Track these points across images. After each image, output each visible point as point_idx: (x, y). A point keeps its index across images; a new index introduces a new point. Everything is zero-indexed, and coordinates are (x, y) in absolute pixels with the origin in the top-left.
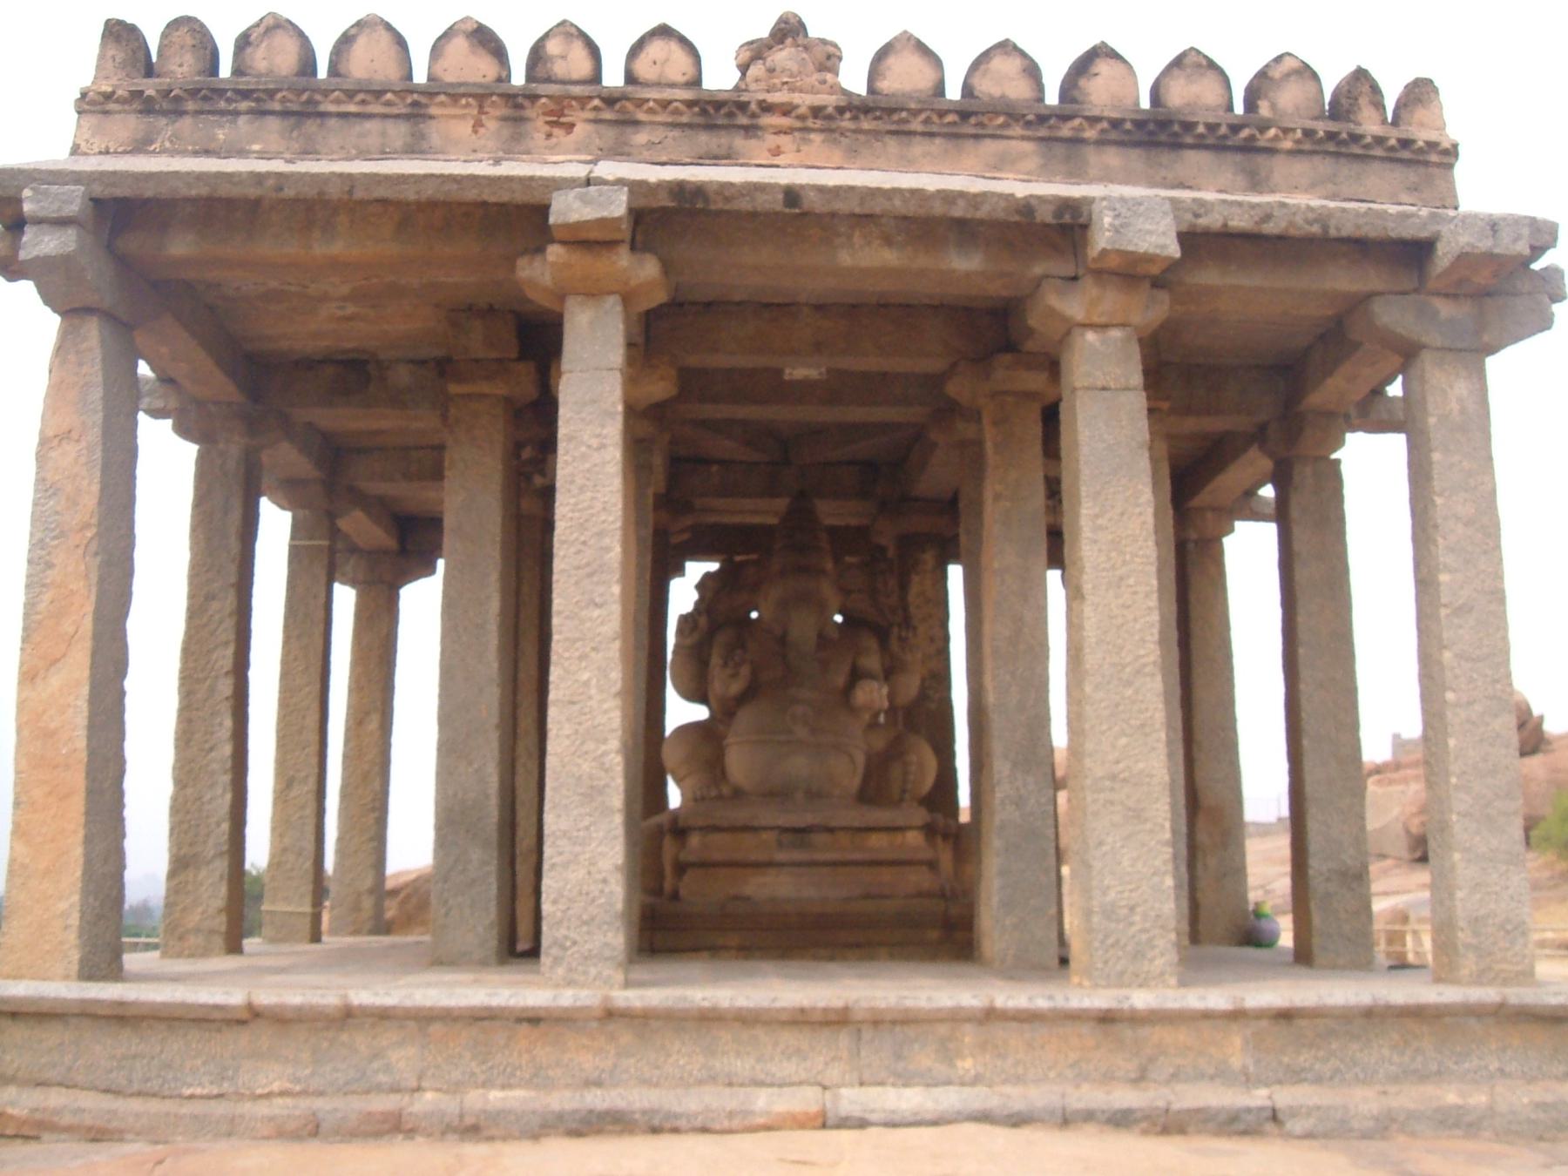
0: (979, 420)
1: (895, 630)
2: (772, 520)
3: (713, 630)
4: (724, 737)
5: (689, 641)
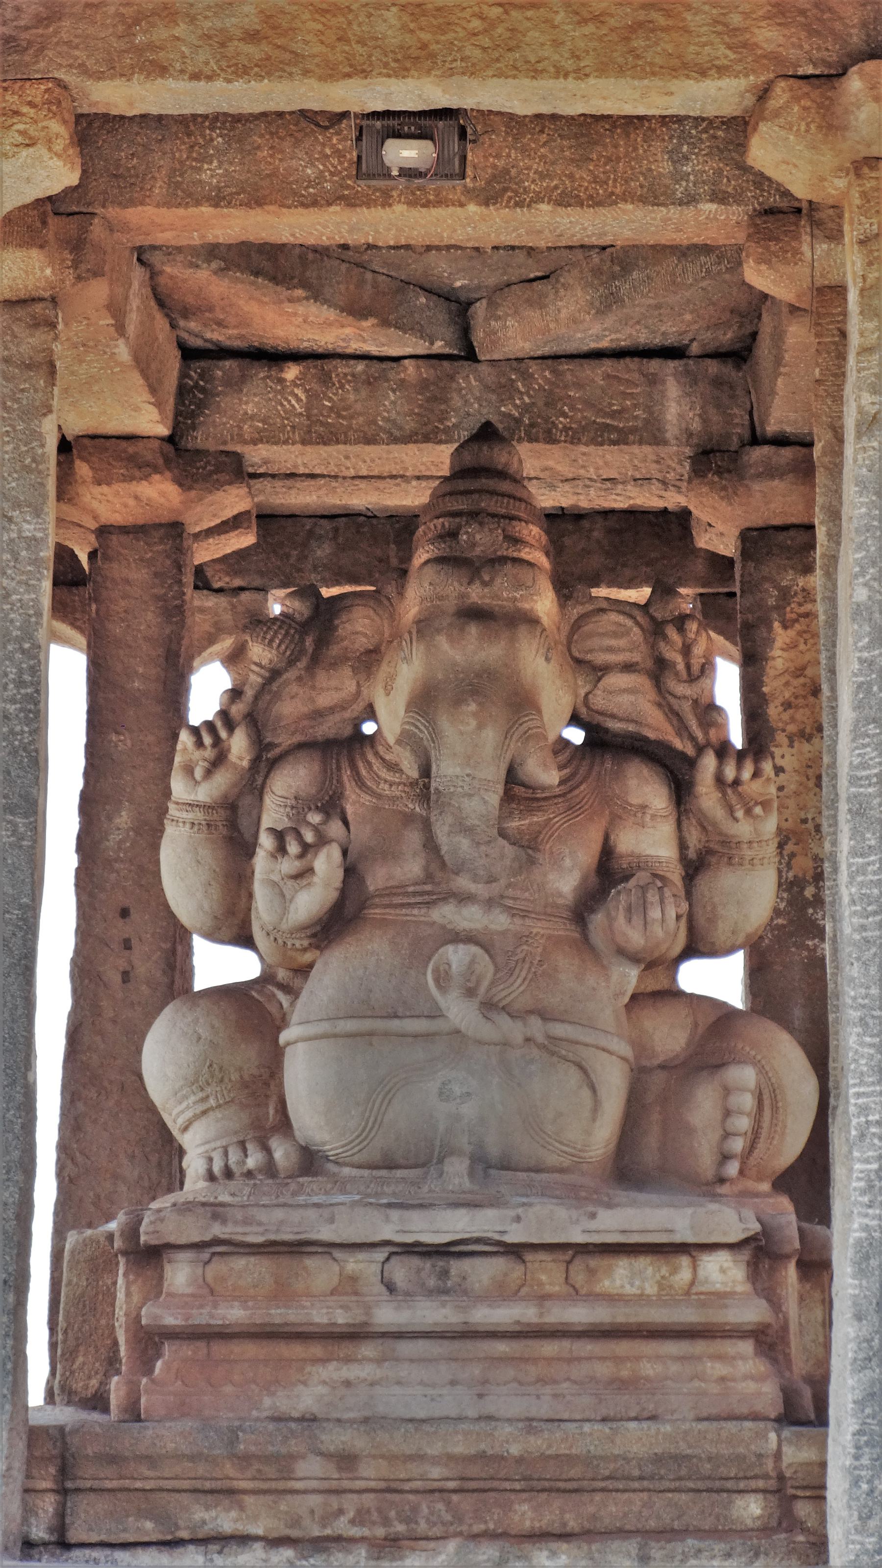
0: (835, 236)
1: (709, 762)
2: (413, 497)
3: (265, 761)
4: (283, 1023)
5: (204, 793)
